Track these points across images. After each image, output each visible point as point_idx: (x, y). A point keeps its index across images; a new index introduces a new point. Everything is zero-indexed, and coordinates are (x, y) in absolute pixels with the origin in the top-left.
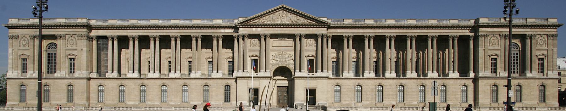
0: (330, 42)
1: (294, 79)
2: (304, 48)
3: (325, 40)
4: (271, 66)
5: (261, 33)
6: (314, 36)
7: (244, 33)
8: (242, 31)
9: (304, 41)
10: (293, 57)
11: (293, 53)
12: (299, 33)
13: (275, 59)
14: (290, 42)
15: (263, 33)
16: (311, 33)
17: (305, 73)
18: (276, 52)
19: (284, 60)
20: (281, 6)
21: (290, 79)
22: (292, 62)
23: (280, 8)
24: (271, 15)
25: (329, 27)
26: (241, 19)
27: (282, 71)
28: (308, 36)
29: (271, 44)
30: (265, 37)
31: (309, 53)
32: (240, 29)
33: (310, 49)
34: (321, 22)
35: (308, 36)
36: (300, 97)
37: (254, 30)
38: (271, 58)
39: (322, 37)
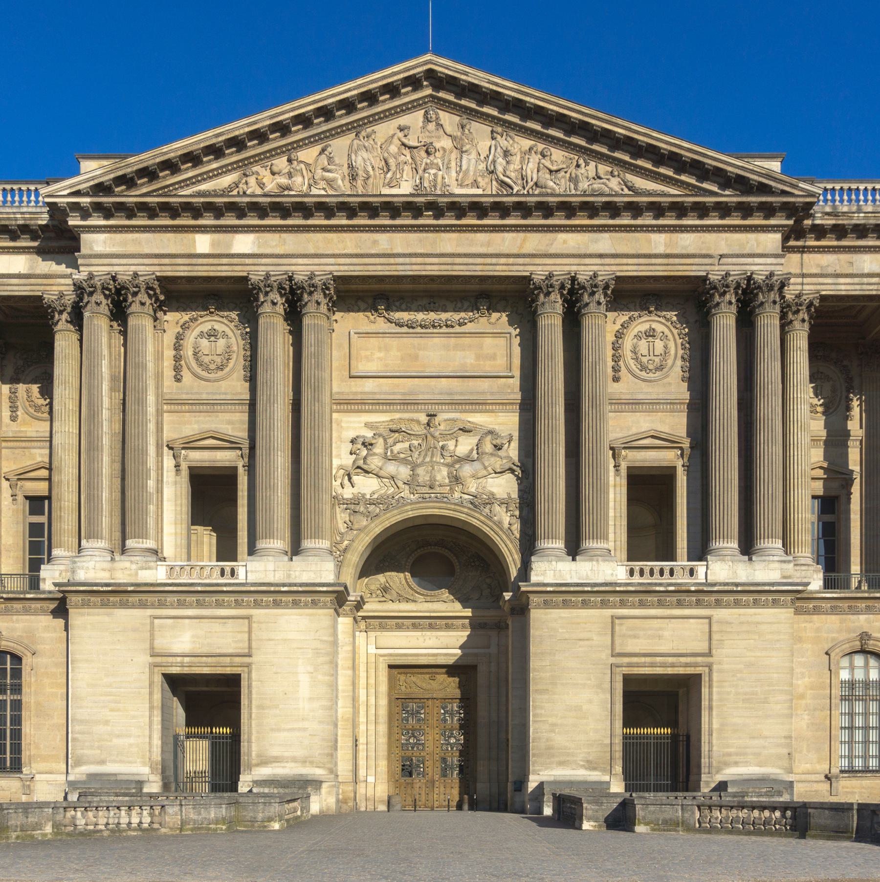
0: (800, 340)
1: (521, 609)
2: (603, 384)
3: (768, 324)
4: (342, 517)
5: (256, 272)
6: (688, 298)
7: (124, 270)
8: (111, 250)
9: (604, 326)
10: (513, 451)
11: (508, 423)
12: (561, 269)
13: (375, 462)
14: (487, 345)
15: (278, 270)
16: (658, 269)
17: (607, 564)
18: (381, 418)
19: (442, 475)
20: (416, 65)
21: (490, 614)
22: (505, 486)
23: (414, 82)
24: (340, 145)
25: (800, 228)
26: (93, 169)
27: (432, 550)
28: (634, 294)
29: (337, 357)
30: (294, 300)
31: (640, 423)
32: (96, 243)
33: (646, 392)
34: (741, 184)
35: (634, 294)
36: (573, 730)
37: (203, 249)
38: (341, 457)
39: (749, 297)
